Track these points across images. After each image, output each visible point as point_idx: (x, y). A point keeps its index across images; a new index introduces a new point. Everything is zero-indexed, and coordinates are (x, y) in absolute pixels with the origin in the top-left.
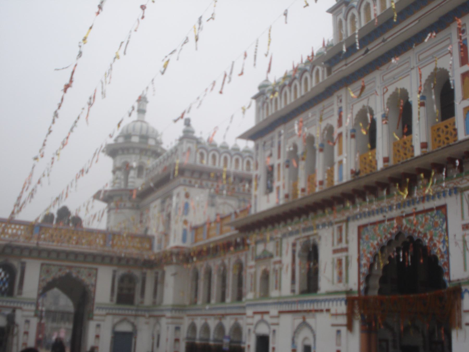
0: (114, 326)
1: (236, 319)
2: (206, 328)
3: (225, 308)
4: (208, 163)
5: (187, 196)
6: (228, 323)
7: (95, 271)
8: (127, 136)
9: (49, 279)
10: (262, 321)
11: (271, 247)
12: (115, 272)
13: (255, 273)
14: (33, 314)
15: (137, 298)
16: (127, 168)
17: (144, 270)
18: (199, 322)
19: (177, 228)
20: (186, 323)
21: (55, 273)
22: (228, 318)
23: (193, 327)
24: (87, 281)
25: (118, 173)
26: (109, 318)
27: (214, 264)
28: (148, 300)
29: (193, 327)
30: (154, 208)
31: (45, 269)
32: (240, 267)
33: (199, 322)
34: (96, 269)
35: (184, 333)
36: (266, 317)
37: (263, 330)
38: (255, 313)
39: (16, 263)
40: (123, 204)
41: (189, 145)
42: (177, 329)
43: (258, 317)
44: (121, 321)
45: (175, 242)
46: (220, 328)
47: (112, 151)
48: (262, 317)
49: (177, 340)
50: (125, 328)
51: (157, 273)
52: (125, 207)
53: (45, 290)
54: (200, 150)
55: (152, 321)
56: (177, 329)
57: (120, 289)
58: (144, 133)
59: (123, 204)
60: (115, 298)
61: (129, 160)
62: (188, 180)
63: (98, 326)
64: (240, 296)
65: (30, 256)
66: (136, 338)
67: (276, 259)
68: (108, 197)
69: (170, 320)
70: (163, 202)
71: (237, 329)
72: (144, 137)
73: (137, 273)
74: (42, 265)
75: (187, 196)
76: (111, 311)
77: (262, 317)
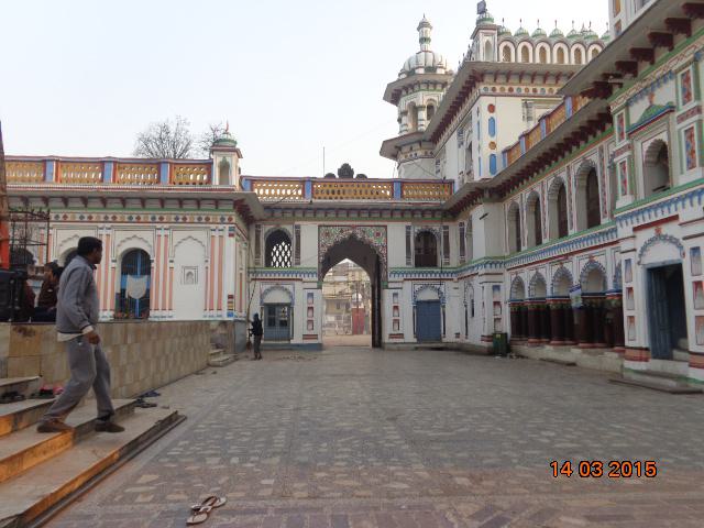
0: (415, 294)
1: (591, 257)
2: (539, 282)
3: (568, 244)
4: (517, 57)
5: (492, 108)
6: (576, 267)
7: (383, 229)
8: (410, 72)
9: (331, 243)
10: (659, 237)
11: (667, 94)
12: (408, 228)
13: (631, 158)
14: (315, 285)
15: (441, 259)
16: (415, 109)
17: (445, 224)
18: (527, 276)
19: (482, 155)
20: (507, 281)
21: (337, 235)
22: (575, 258)
23: (519, 284)
24: (375, 242)
25: (404, 119)
26: (408, 285)
27: (543, 186)
28: (454, 259)
29: (519, 284)
30: (451, 144)
31: (323, 232)
32: (590, 175)
33: (527, 276)
34: (386, 227)
35: (505, 295)
36: (666, 229)
37: (662, 254)
38: (635, 229)
39: (289, 229)
40: (413, 153)
41: (490, 39)
42: (496, 288)
43: (651, 233)
44: (421, 290)
45: (482, 173)
46: (564, 277)
47: (394, 95)
48: (658, 231)
49: (497, 303)
50: (429, 295)
51: (462, 224)
52: (417, 157)
53: (329, 260)
54: (504, 44)
55: (461, 284)
56: (496, 288)
57: (417, 249)
58: (430, 63)
59: (413, 153)
60: (413, 261)
61: (414, 100)
62: (490, 87)
63: (395, 295)
64: (593, 219)
65: (304, 218)
66: (444, 307)
67: (693, 104)
68: (392, 149)
69: (484, 278)
70: (460, 133)
71: (595, 272)
72: (431, 69)
73: (436, 227)
74: (320, 226)
75: (492, 108)
76: (409, 277)
77: (658, 231)
